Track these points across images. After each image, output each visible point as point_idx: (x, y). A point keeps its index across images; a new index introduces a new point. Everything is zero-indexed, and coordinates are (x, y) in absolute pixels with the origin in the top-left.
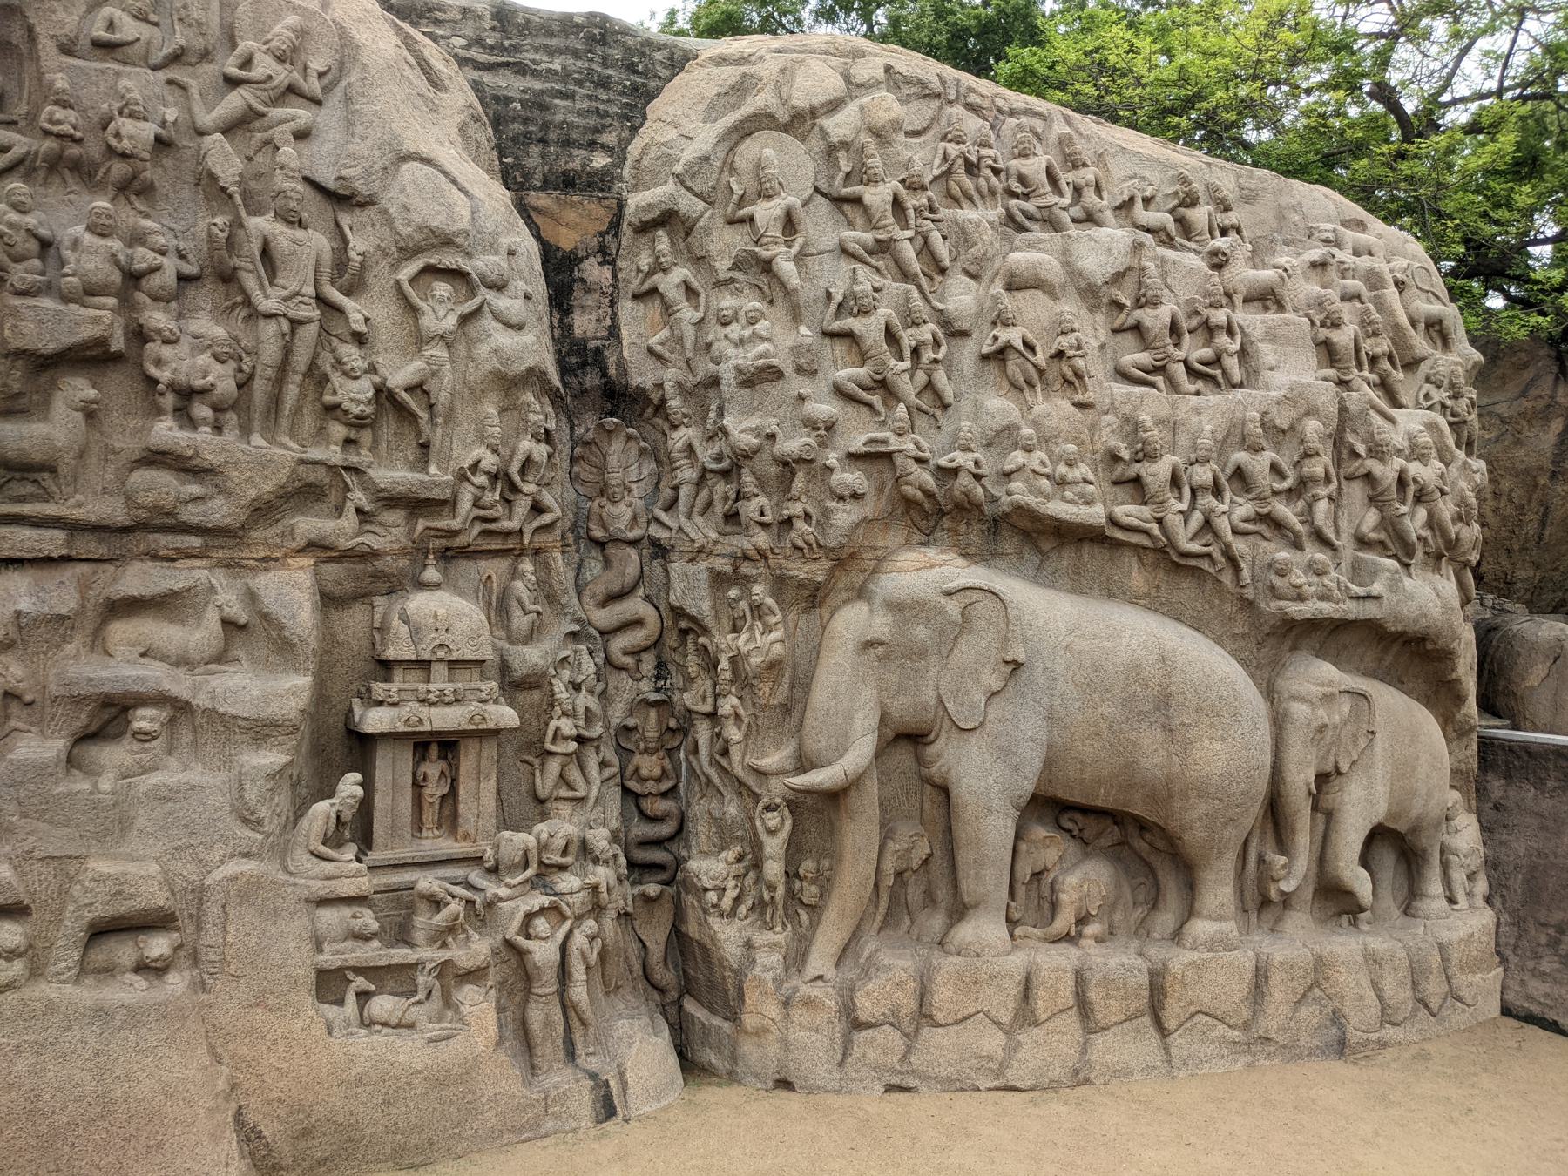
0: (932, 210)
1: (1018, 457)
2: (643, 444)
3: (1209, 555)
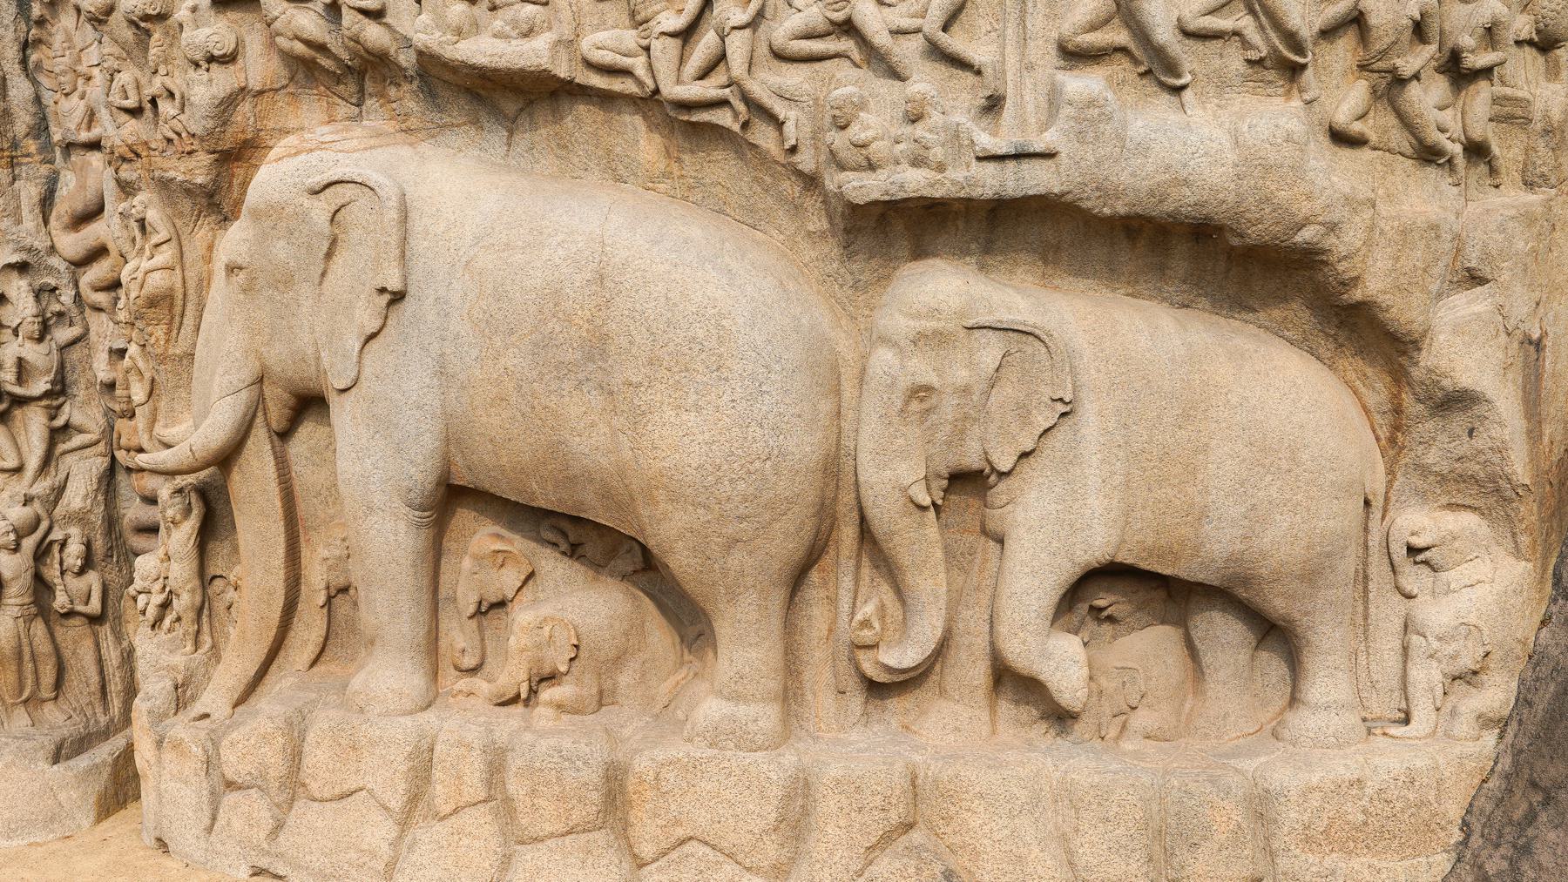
3: (723, 103)
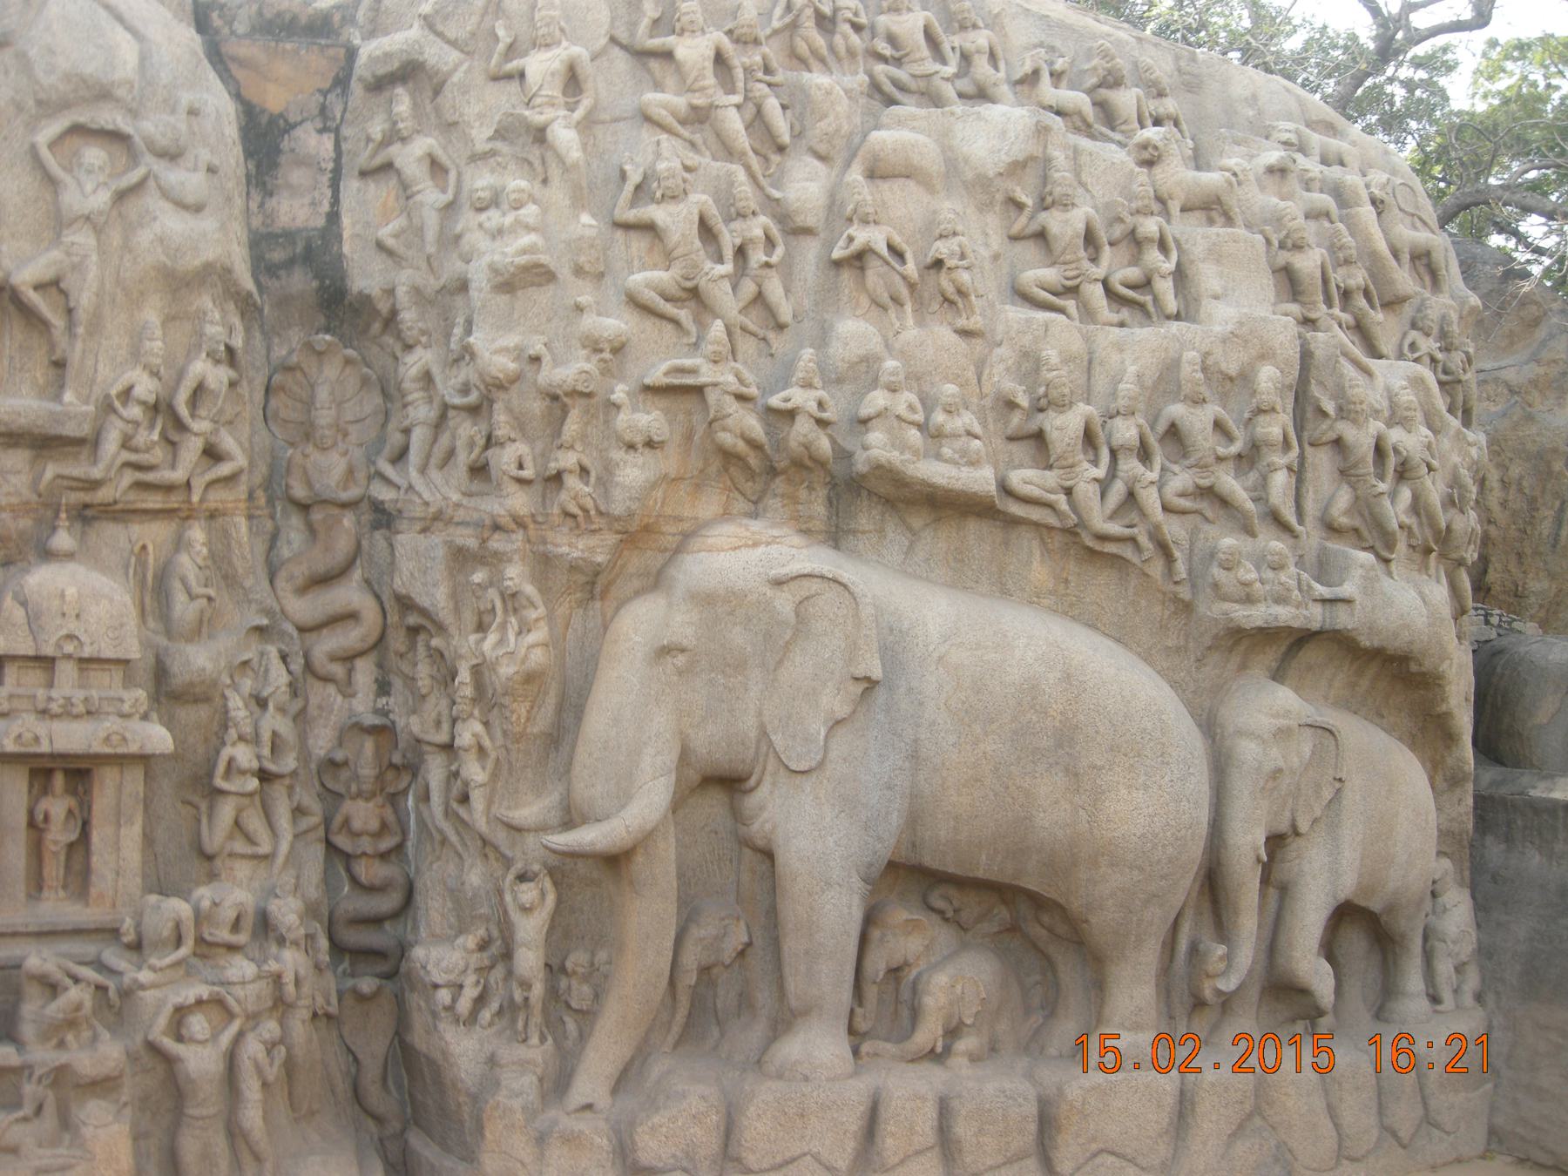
0: (767, 70)
2: (365, 370)
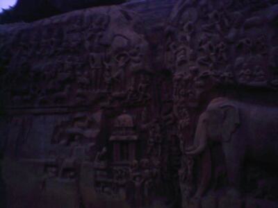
1: (242, 71)
